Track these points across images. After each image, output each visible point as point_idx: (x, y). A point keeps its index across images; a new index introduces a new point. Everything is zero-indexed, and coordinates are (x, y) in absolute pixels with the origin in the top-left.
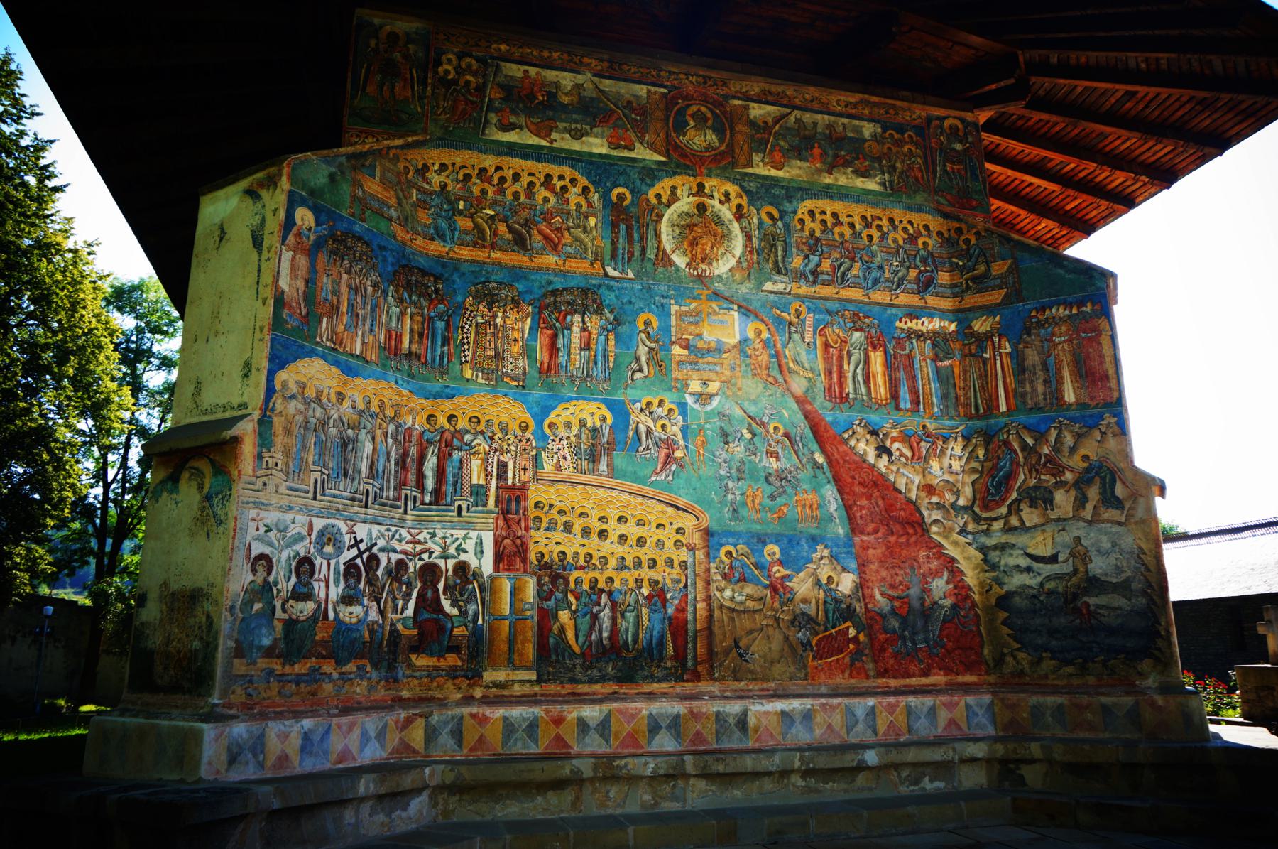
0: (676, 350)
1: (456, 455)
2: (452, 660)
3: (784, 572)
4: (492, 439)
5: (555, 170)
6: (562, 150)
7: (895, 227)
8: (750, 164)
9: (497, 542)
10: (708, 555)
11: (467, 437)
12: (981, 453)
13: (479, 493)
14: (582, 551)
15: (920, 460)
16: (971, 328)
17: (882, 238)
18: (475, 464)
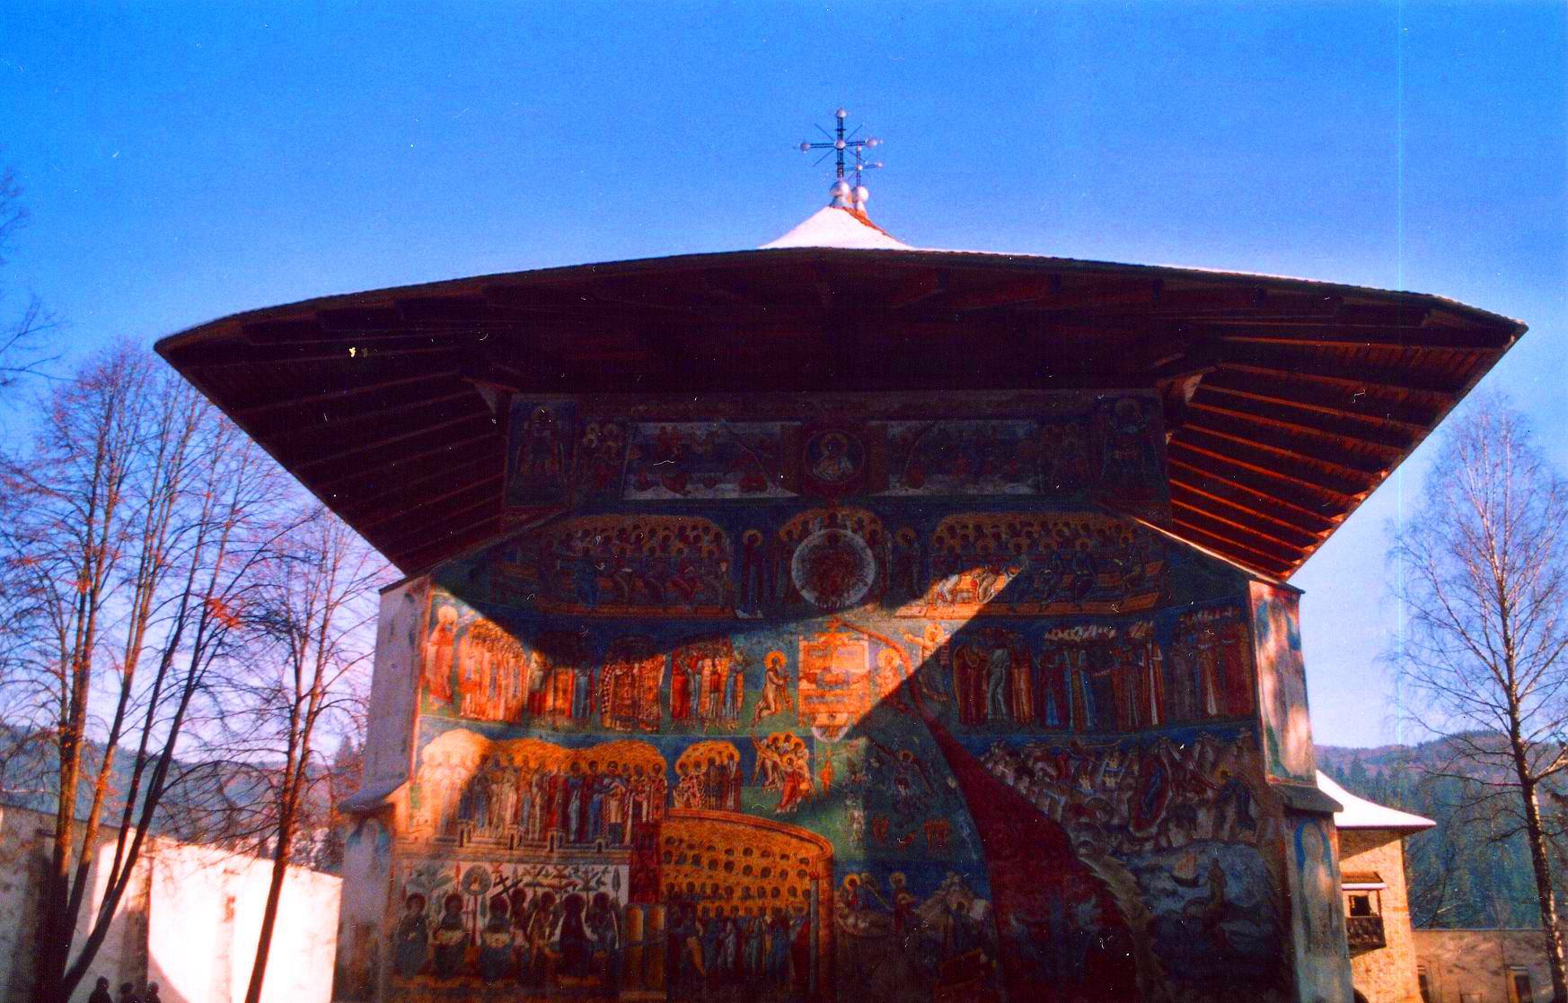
0: (804, 685)
1: (596, 797)
2: (591, 980)
3: (909, 898)
4: (628, 781)
5: (688, 520)
6: (695, 501)
7: (1048, 532)
8: (886, 486)
9: (632, 876)
10: (831, 884)
11: (606, 781)
12: (1136, 768)
13: (617, 831)
14: (709, 883)
15: (1067, 780)
16: (1128, 633)
17: (1030, 547)
18: (614, 804)
